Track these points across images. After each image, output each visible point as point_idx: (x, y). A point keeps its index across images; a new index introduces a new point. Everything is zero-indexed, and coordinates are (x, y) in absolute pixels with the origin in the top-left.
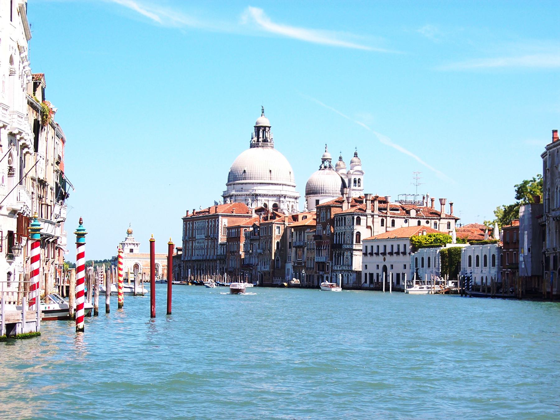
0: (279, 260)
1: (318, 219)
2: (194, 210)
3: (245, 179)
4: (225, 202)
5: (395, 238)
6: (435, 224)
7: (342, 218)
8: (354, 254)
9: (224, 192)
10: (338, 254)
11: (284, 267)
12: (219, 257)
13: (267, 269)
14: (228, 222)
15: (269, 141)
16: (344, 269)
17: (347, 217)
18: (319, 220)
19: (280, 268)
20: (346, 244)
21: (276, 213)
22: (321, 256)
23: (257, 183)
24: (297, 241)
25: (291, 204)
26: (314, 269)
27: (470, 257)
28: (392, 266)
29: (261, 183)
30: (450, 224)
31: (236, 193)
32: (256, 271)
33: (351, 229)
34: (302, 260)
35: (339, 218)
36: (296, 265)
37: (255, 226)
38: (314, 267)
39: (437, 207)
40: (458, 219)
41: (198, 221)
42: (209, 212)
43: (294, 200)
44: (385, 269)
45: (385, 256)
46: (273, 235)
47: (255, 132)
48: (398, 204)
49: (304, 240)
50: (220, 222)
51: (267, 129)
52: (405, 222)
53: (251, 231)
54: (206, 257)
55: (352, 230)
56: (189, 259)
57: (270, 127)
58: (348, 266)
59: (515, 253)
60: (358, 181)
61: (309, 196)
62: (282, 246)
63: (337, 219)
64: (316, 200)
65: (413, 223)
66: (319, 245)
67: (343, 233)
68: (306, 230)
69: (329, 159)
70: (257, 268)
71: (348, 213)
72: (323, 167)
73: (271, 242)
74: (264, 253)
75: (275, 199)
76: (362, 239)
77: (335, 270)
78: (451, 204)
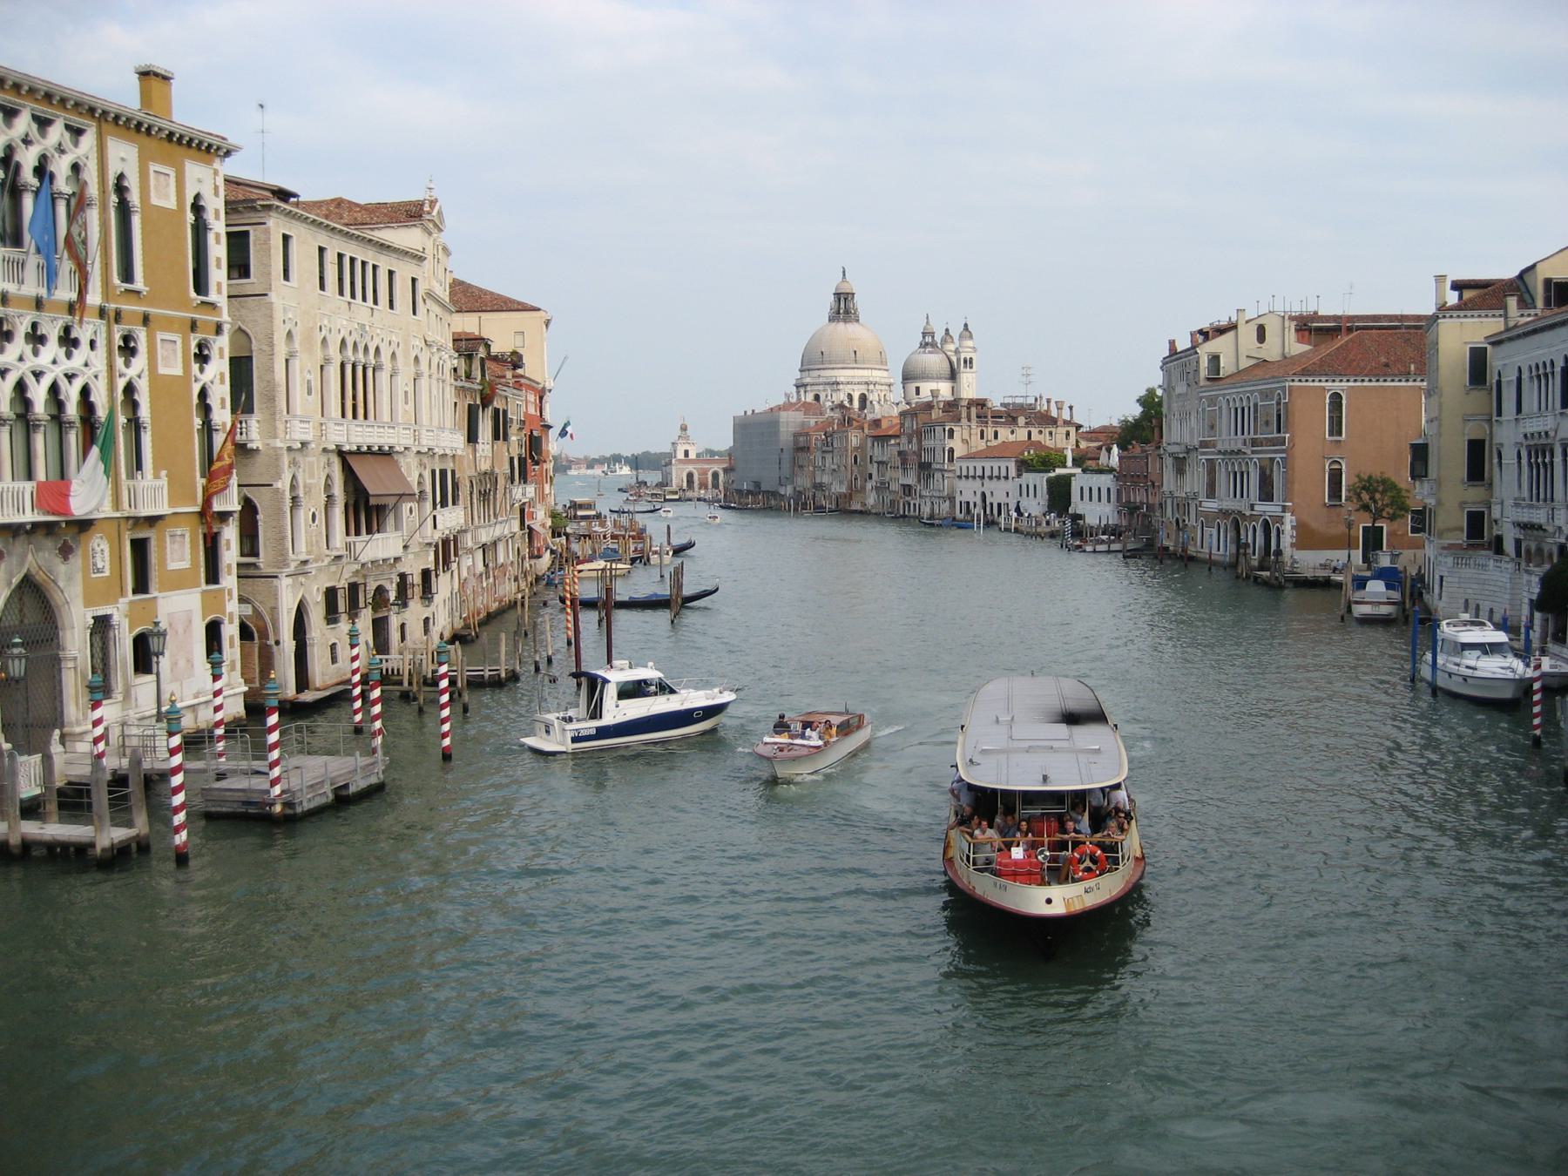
3: (822, 363)
4: (798, 392)
6: (1051, 433)
11: (863, 488)
13: (844, 490)
27: (1082, 488)
39: (1054, 413)
40: (1081, 426)
43: (887, 388)
44: (984, 495)
48: (1004, 409)
57: (853, 294)
62: (862, 460)
66: (904, 462)
75: (865, 387)
78: (1071, 408)
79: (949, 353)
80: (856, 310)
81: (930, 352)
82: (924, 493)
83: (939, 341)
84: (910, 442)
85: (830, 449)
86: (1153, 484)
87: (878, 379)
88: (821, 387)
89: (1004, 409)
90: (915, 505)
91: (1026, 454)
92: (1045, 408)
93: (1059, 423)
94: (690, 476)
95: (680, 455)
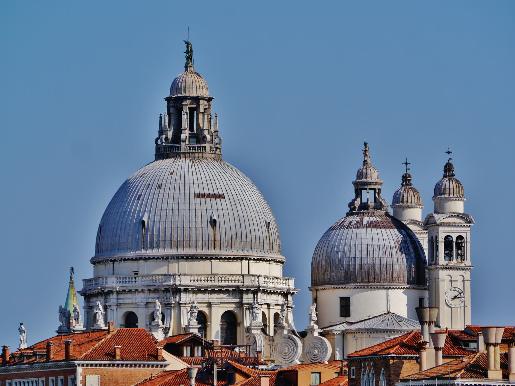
4: (89, 309)
9: (86, 281)
15: (208, 137)
25: (272, 312)
41: (18, 381)
43: (280, 299)
47: (169, 114)
51: (203, 104)
57: (209, 100)
60: (457, 243)
64: (342, 299)
69: (376, 184)
72: (357, 203)
79: (411, 227)
81: (372, 225)
87: (262, 283)
88: (139, 298)
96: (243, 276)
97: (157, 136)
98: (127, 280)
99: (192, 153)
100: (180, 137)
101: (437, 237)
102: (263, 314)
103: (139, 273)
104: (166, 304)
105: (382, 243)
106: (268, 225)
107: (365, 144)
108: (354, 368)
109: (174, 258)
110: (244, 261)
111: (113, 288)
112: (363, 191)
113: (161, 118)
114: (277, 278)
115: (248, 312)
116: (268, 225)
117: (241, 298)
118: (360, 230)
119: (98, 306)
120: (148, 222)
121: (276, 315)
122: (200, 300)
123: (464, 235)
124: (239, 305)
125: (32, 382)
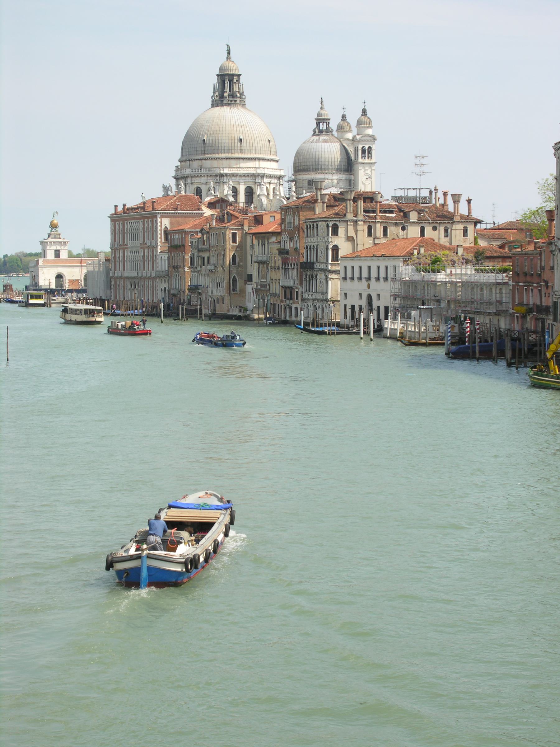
0: (236, 280)
1: (283, 226)
2: (124, 205)
4: (178, 185)
5: (381, 256)
6: (446, 231)
7: (313, 224)
8: (329, 276)
10: (309, 276)
11: (243, 291)
12: (158, 273)
13: (221, 293)
14: (171, 223)
15: (238, 95)
16: (317, 297)
17: (320, 224)
18: (285, 227)
19: (238, 291)
20: (320, 263)
21: (231, 214)
22: (289, 278)
23: (222, 159)
24: (259, 253)
25: (272, 186)
26: (279, 296)
28: (378, 295)
29: (227, 159)
30: (467, 230)
31: (192, 173)
32: (206, 295)
33: (326, 242)
34: (266, 282)
35: (310, 225)
36: (259, 287)
37: (203, 231)
38: (279, 294)
40: (480, 222)
41: (129, 221)
42: (143, 208)
43: (276, 181)
44: (370, 297)
45: (369, 282)
46: (228, 246)
47: (219, 83)
49: (268, 254)
50: (159, 224)
52: (402, 229)
53: (198, 239)
54: (142, 273)
55: (327, 243)
56: (120, 275)
57: (239, 76)
58: (323, 293)
59: (526, 289)
61: (297, 174)
62: (241, 260)
63: (307, 225)
65: (414, 231)
66: (285, 262)
67: (315, 247)
68: (271, 238)
69: (327, 119)
70: (207, 290)
71: (320, 218)
73: (224, 255)
74: (216, 270)
76: (339, 257)
77: (306, 299)
78: (469, 201)
80: (242, 94)
82: (306, 296)
83: (335, 129)
84: (291, 239)
85: (206, 247)
86: (546, 282)
87: (266, 172)
88: (203, 180)
89: (394, 203)
90: (296, 308)
91: (416, 252)
92: (441, 201)
93: (457, 218)
94: (59, 277)
95: (50, 255)
96: (256, 168)
97: (212, 94)
98: (196, 170)
99: (230, 104)
100: (224, 95)
101: (358, 147)
102: (267, 188)
103: (202, 167)
104: (216, 183)
105: (329, 150)
106: (270, 141)
107: (321, 98)
108: (283, 213)
109: (220, 159)
110: (257, 160)
111: (189, 174)
112: (320, 123)
113: (214, 85)
114: (274, 169)
115: (259, 186)
116: (270, 141)
117: (255, 179)
118: (318, 144)
119: (181, 184)
120: (207, 140)
121: (274, 189)
122: (233, 181)
123: (372, 146)
124: (254, 183)
125: (137, 222)
